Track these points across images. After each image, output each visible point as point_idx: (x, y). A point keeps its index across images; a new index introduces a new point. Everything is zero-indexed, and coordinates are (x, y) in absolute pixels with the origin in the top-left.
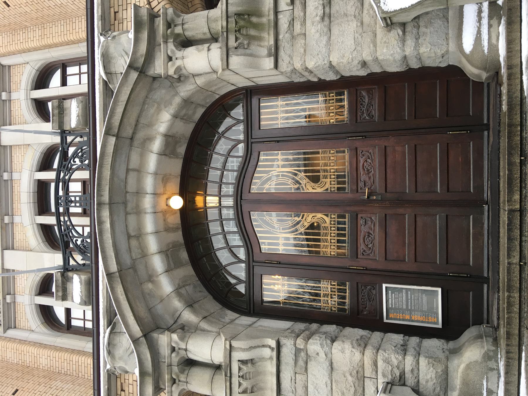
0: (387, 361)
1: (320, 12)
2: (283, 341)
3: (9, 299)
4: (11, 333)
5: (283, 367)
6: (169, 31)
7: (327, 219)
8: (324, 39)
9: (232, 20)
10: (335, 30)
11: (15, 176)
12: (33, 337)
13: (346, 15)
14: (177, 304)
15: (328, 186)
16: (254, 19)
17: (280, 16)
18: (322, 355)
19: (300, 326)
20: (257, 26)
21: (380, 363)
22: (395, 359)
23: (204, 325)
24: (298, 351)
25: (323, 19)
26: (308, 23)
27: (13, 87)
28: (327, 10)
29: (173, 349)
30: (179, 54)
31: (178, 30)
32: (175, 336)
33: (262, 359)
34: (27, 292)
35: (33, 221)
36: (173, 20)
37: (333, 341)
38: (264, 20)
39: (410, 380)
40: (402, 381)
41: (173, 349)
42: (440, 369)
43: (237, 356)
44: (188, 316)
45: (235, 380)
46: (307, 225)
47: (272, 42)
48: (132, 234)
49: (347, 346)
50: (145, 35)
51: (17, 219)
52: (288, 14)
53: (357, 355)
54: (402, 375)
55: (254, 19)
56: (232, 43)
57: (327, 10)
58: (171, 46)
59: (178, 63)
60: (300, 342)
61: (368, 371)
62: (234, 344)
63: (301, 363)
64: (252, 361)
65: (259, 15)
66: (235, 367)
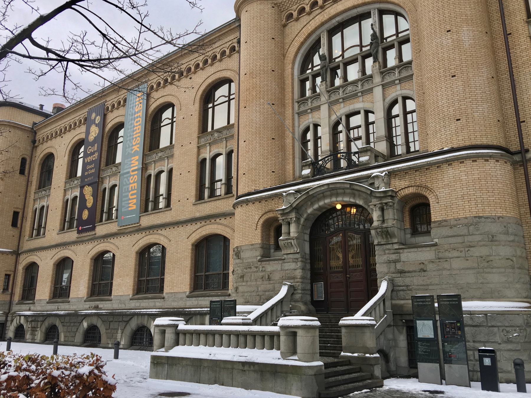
0: (299, 285)
1: (391, 259)
2: (300, 254)
3: (309, 111)
4: (296, 116)
5: (293, 255)
6: (384, 204)
7: (341, 263)
8: (382, 262)
9: (385, 229)
10: (385, 265)
11: (361, 99)
12: (296, 129)
13: (390, 268)
14: (305, 216)
15: (351, 262)
16: (388, 236)
17: (391, 245)
18: (298, 267)
19: (308, 257)
20: (386, 237)
21: (298, 283)
22: (300, 287)
23: (300, 226)
24: (297, 259)
25: (389, 260)
26: (388, 255)
27: (403, 84)
28: (392, 262)
29: (291, 219)
30: (377, 209)
31: (385, 208)
32: (294, 219)
33: (294, 248)
34: (313, 120)
35: (341, 115)
36: (388, 205)
37: (302, 269)
38: (390, 239)
39: (295, 292)
40: (295, 290)
41: (291, 219)
42: (299, 300)
43: (292, 241)
44: (302, 220)
45: (286, 241)
46: (339, 255)
47: (382, 243)
48: (324, 194)
49: (301, 274)
50: (382, 195)
51: (342, 105)
52: (392, 248)
53: (299, 277)
54: (296, 290)
55: (388, 236)
56: (379, 230)
57: (392, 262)
58: (379, 206)
59: (374, 209)
60: (300, 259)
61: (296, 280)
62: (295, 240)
63: (295, 260)
64: (292, 246)
65: (391, 237)
66: (289, 241)
